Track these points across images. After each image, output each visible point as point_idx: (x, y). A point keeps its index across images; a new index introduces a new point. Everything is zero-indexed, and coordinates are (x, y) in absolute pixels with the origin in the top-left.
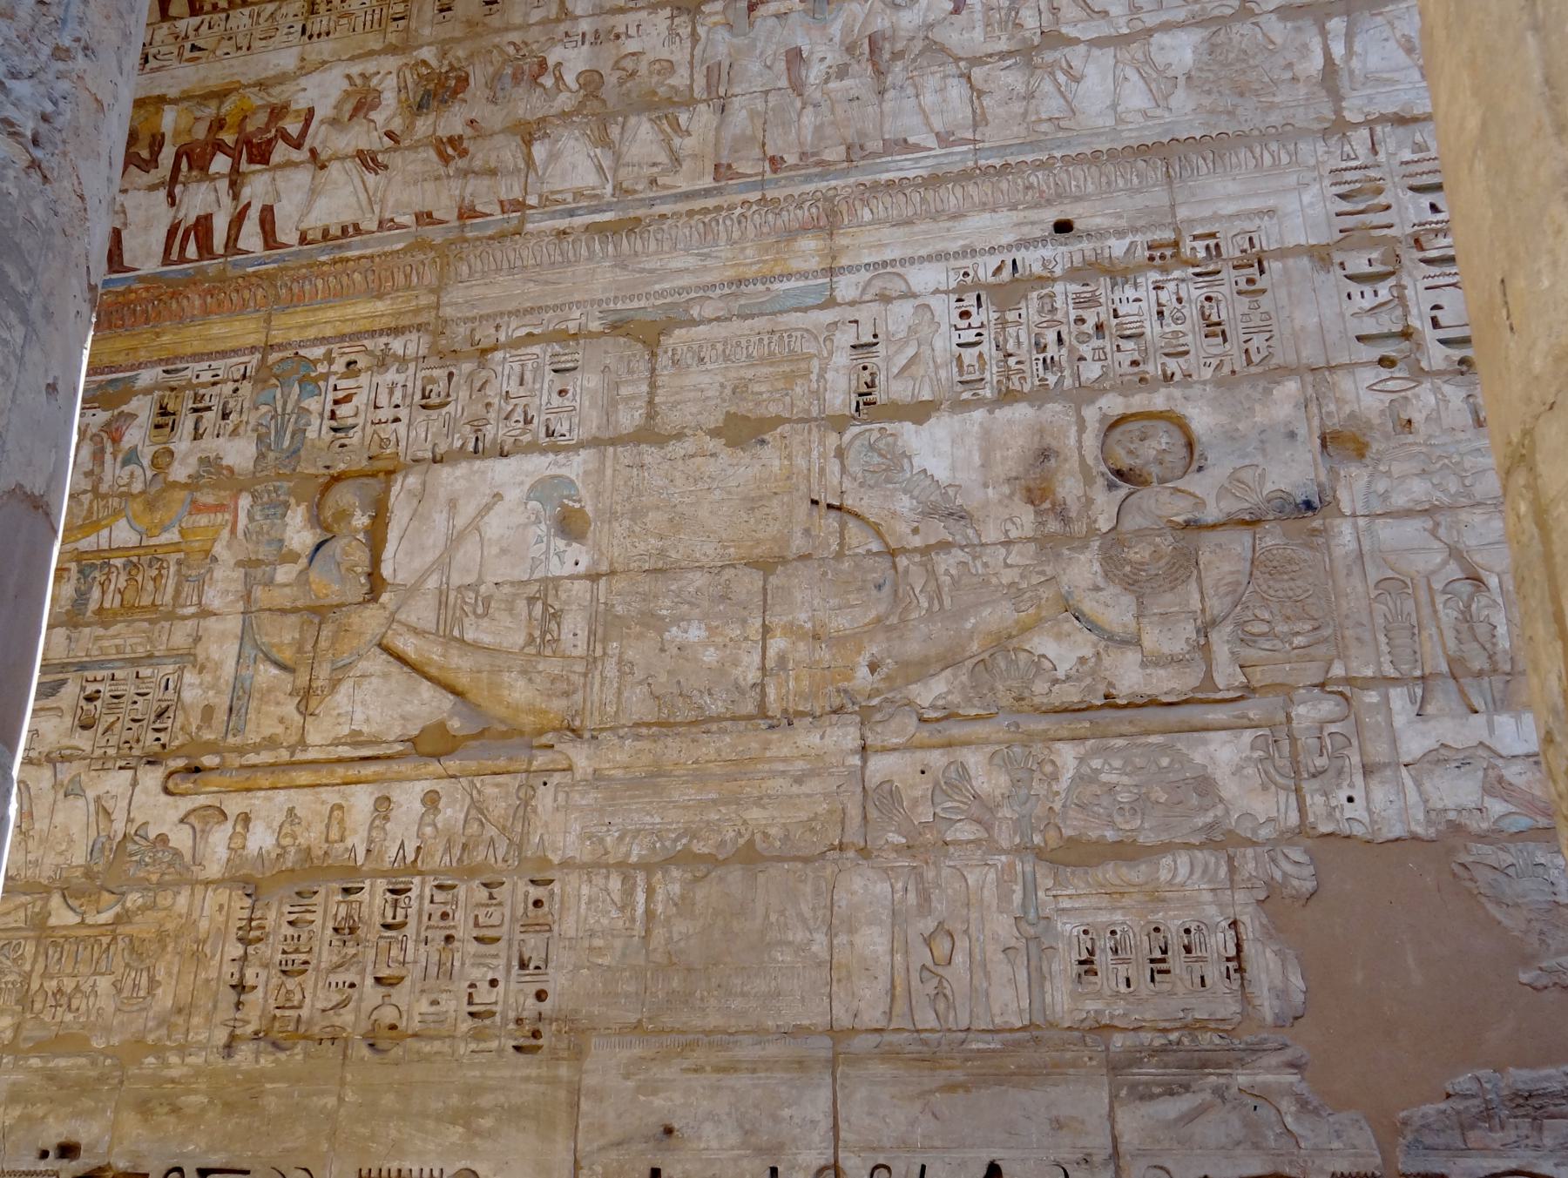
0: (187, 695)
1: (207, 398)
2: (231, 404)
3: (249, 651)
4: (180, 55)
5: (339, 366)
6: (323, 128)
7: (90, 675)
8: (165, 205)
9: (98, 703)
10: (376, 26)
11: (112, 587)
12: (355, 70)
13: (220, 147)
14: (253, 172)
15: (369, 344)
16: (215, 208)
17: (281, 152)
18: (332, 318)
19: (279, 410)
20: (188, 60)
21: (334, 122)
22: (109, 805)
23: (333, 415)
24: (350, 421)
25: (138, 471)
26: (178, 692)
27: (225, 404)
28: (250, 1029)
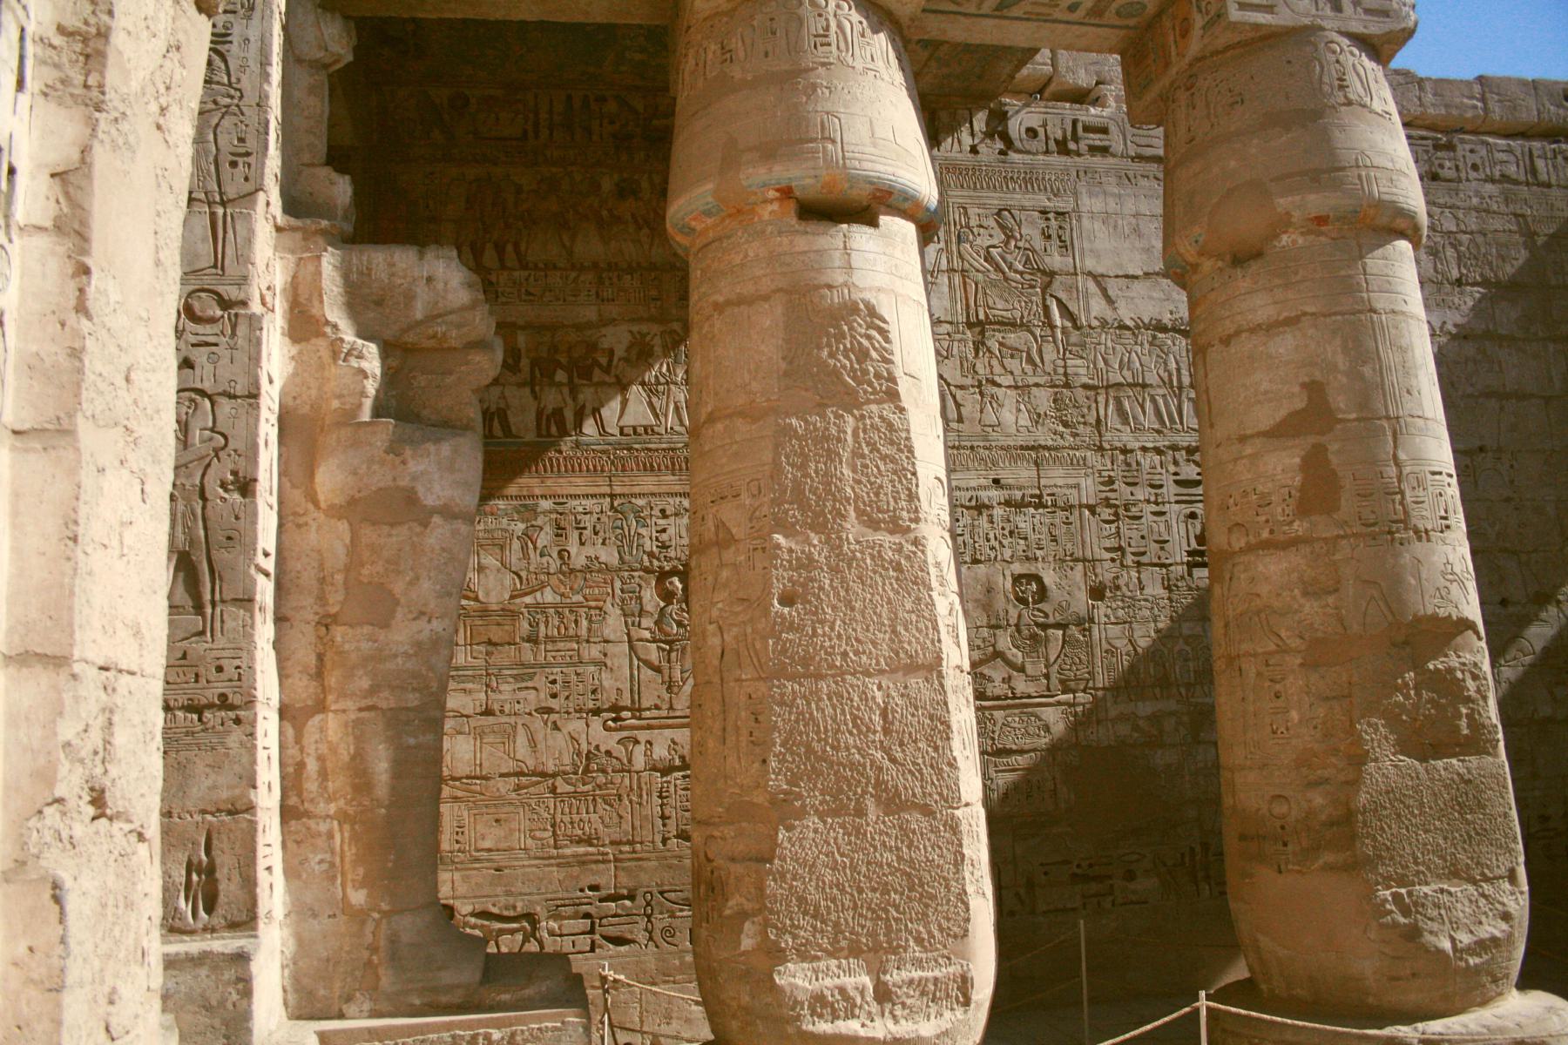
0: (605, 683)
3: (636, 662)
5: (656, 512)
8: (531, 399)
12: (635, 329)
13: (559, 365)
15: (671, 500)
17: (597, 375)
18: (648, 483)
21: (626, 360)
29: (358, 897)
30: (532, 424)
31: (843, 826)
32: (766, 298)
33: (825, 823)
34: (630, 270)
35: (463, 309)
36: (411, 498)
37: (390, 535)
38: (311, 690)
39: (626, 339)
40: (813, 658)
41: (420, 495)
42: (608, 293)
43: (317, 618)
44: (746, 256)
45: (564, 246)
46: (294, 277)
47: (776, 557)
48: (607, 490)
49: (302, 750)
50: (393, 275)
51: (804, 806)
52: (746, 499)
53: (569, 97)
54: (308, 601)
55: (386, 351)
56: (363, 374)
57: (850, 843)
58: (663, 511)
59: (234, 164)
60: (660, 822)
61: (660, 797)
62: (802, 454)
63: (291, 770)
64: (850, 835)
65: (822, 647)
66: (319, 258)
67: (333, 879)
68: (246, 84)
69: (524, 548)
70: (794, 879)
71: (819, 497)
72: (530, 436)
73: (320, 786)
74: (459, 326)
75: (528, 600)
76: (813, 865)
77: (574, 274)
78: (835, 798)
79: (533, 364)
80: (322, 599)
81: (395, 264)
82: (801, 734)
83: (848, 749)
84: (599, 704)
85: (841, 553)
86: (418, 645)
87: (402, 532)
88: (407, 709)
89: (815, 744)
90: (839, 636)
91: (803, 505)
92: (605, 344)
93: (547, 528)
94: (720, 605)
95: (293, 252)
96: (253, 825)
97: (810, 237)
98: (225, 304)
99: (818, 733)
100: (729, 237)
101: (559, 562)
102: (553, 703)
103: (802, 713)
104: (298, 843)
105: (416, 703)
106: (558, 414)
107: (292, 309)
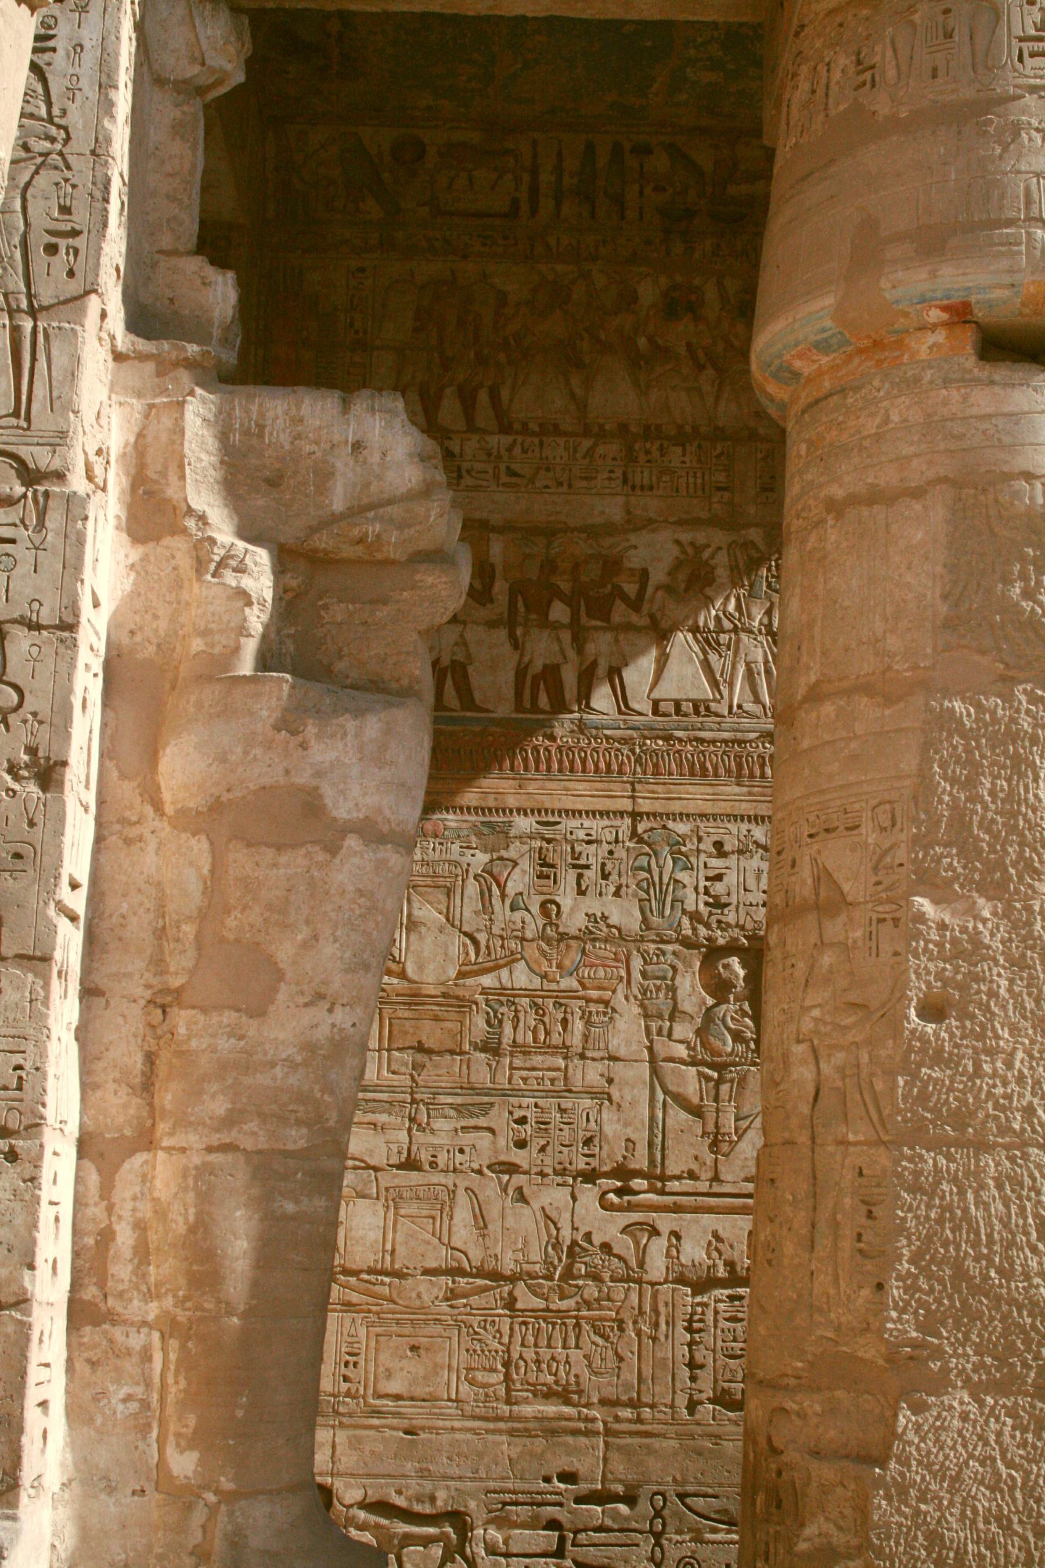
0: (609, 1129)
1: (584, 855)
2: (609, 867)
3: (660, 1096)
4: (496, 477)
5: (707, 845)
6: (659, 594)
7: (514, 1100)
8: (507, 647)
9: (528, 1127)
10: (700, 492)
11: (521, 1024)
12: (685, 537)
13: (556, 593)
14: (597, 629)
15: (733, 827)
16: (561, 661)
17: (620, 613)
18: (695, 796)
19: (657, 879)
20: (504, 485)
22: (554, 1215)
23: (707, 892)
24: (723, 900)
25: (528, 918)
26: (599, 1123)
27: (603, 865)
28: (704, 1396)
29: (184, 1464)
30: (509, 692)
31: (1012, 1413)
32: (917, 493)
33: (981, 1403)
34: (681, 439)
35: (410, 496)
36: (311, 805)
37: (275, 865)
38: (132, 1111)
39: (669, 553)
40: (973, 1114)
41: (328, 802)
42: (643, 476)
43: (148, 994)
44: (887, 420)
45: (573, 395)
46: (140, 436)
47: (917, 935)
48: (626, 805)
49: (110, 1209)
50: (298, 437)
51: (945, 1370)
52: (869, 834)
53: (590, 147)
54: (136, 965)
55: (284, 559)
56: (244, 597)
57: (1024, 1444)
58: (718, 845)
59: (52, 249)
60: (686, 1372)
61: (689, 1329)
62: (970, 762)
63: (90, 1241)
64: (1025, 1430)
65: (990, 1094)
66: (181, 404)
67: (144, 1430)
68: (75, 119)
69: (485, 896)
70: (922, 1499)
71: (996, 837)
72: (504, 710)
73: (135, 1272)
74: (402, 526)
75: (487, 981)
76: (957, 1478)
77: (587, 443)
78: (1001, 1361)
79: (513, 594)
80: (158, 964)
81: (303, 418)
82: (946, 1244)
83: (1027, 1277)
84: (594, 1163)
85: (1030, 935)
86: (310, 1047)
87: (294, 862)
88: (287, 1154)
89: (969, 1263)
90: (1021, 1079)
91: (968, 850)
92: (635, 560)
93: (525, 864)
94: (816, 1013)
95: (139, 395)
96: (24, 1330)
97: (997, 389)
98: (30, 476)
99: (976, 1244)
100: (857, 389)
101: (541, 922)
102: (519, 1157)
103: (950, 1208)
104: (93, 1364)
105: (302, 1144)
106: (551, 674)
107: (134, 487)
